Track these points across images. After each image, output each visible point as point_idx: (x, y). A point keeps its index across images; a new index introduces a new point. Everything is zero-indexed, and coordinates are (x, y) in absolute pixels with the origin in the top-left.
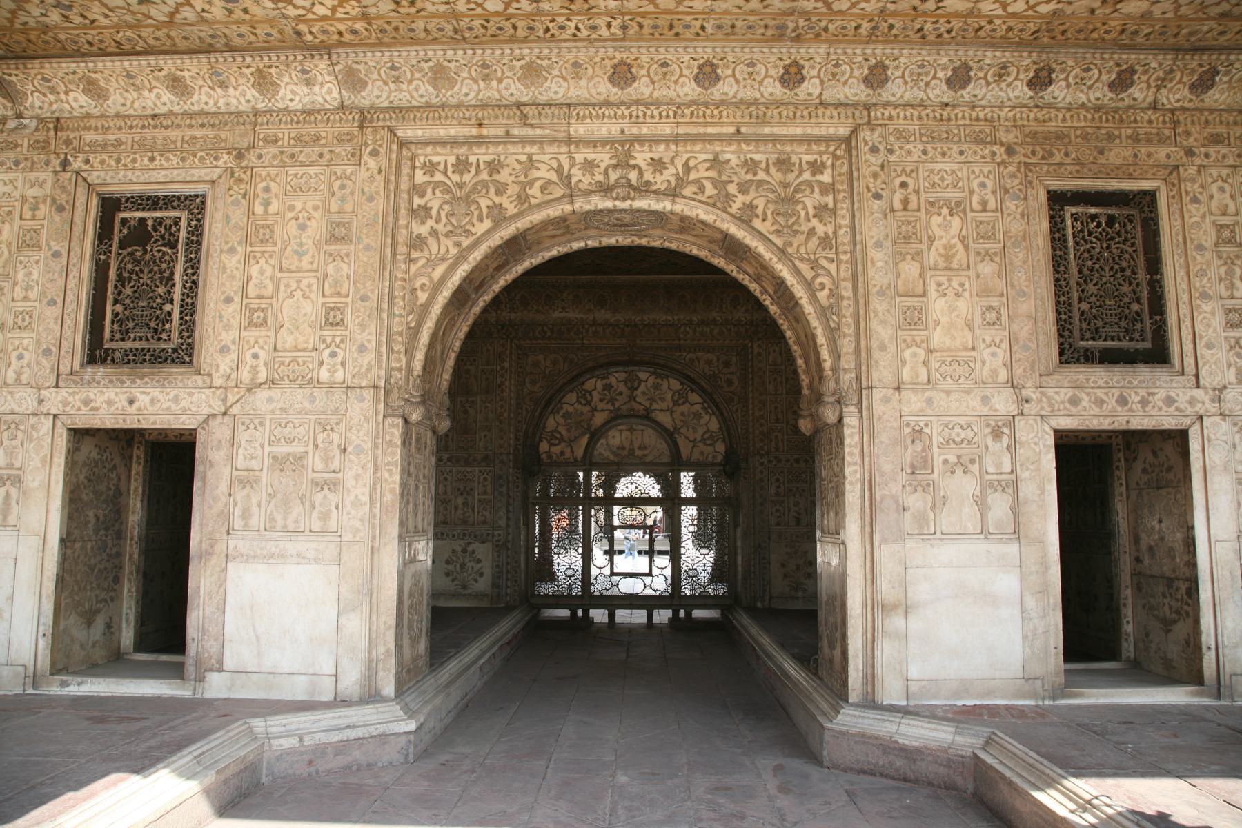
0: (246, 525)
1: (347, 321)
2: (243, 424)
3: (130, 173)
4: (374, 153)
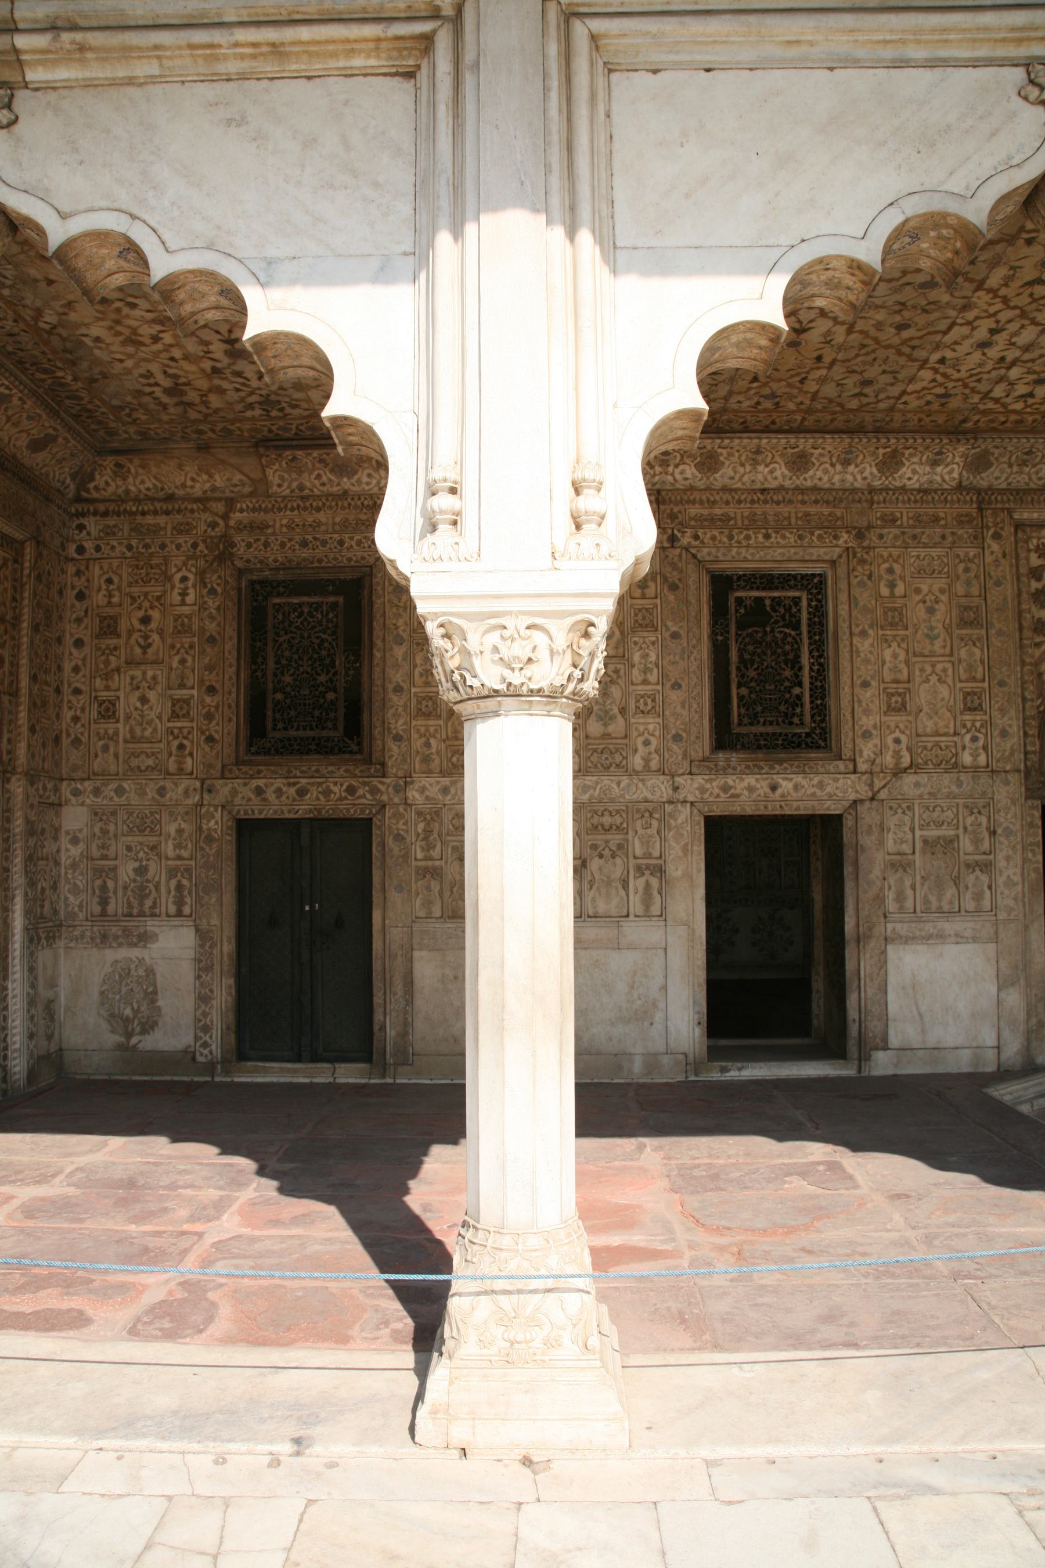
0: (901, 907)
1: (986, 705)
2: (891, 808)
3: (743, 550)
4: (997, 536)
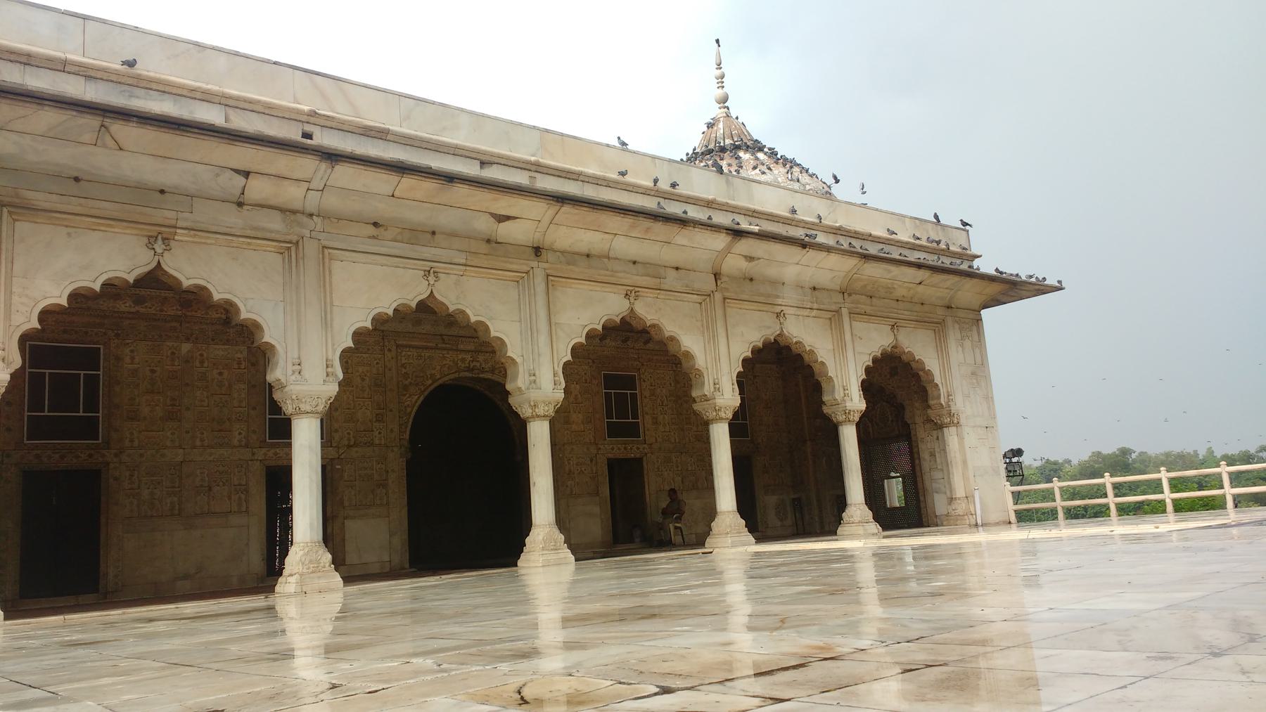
4: (390, 350)
